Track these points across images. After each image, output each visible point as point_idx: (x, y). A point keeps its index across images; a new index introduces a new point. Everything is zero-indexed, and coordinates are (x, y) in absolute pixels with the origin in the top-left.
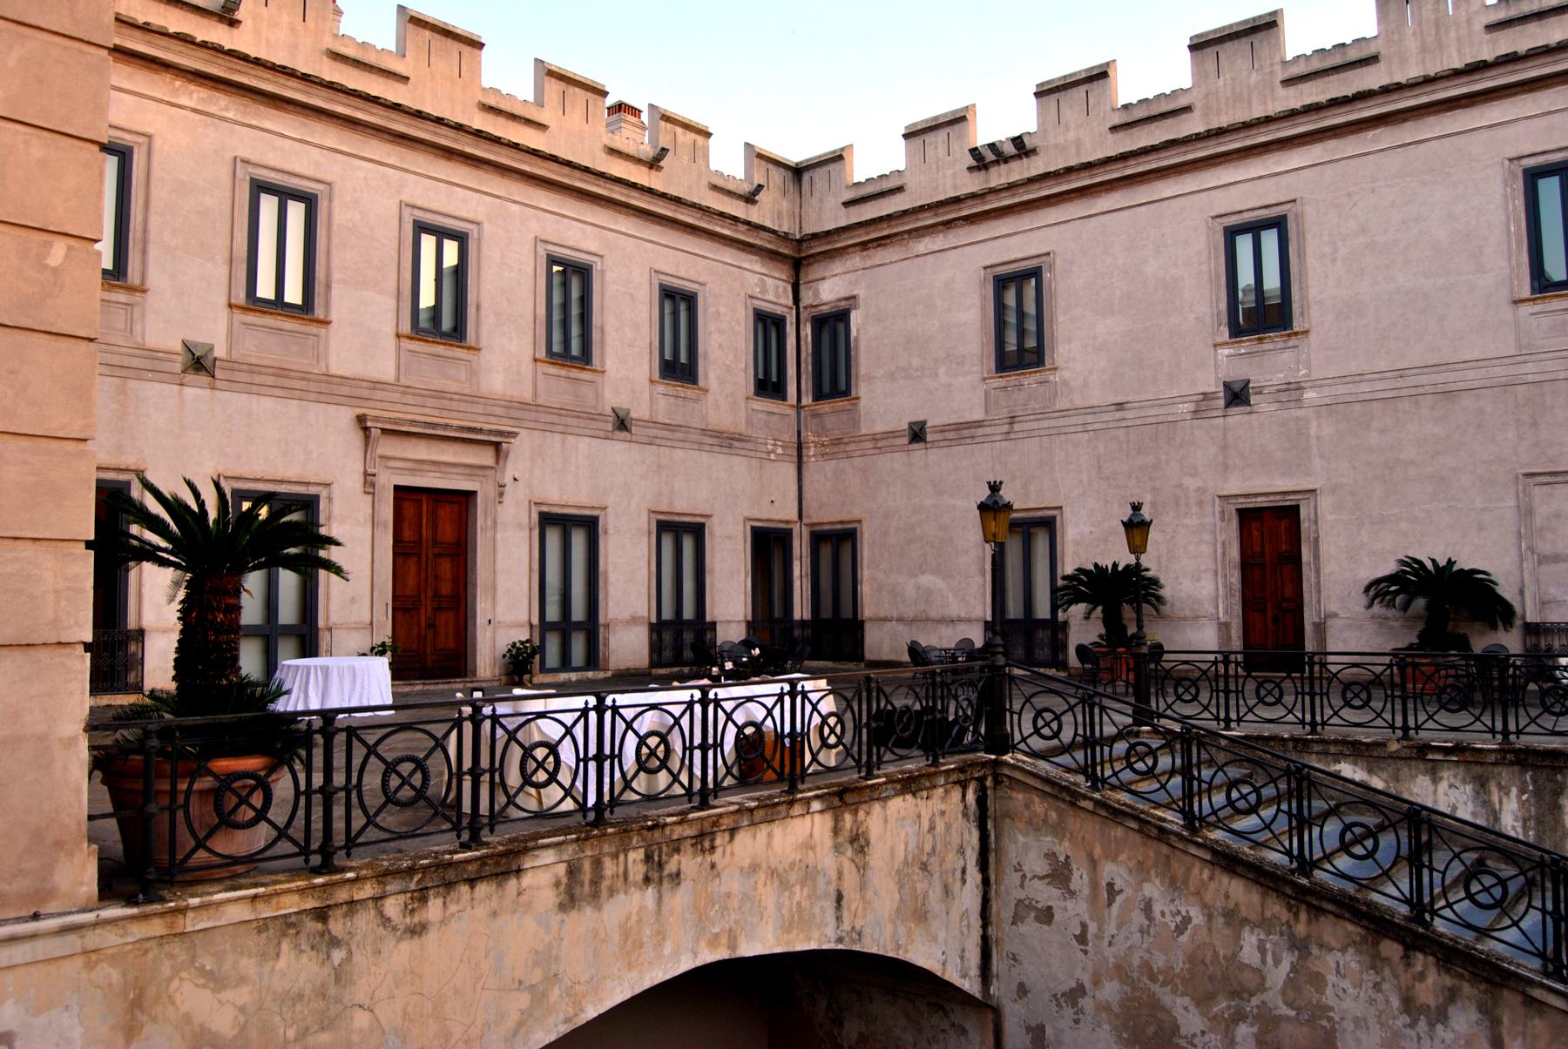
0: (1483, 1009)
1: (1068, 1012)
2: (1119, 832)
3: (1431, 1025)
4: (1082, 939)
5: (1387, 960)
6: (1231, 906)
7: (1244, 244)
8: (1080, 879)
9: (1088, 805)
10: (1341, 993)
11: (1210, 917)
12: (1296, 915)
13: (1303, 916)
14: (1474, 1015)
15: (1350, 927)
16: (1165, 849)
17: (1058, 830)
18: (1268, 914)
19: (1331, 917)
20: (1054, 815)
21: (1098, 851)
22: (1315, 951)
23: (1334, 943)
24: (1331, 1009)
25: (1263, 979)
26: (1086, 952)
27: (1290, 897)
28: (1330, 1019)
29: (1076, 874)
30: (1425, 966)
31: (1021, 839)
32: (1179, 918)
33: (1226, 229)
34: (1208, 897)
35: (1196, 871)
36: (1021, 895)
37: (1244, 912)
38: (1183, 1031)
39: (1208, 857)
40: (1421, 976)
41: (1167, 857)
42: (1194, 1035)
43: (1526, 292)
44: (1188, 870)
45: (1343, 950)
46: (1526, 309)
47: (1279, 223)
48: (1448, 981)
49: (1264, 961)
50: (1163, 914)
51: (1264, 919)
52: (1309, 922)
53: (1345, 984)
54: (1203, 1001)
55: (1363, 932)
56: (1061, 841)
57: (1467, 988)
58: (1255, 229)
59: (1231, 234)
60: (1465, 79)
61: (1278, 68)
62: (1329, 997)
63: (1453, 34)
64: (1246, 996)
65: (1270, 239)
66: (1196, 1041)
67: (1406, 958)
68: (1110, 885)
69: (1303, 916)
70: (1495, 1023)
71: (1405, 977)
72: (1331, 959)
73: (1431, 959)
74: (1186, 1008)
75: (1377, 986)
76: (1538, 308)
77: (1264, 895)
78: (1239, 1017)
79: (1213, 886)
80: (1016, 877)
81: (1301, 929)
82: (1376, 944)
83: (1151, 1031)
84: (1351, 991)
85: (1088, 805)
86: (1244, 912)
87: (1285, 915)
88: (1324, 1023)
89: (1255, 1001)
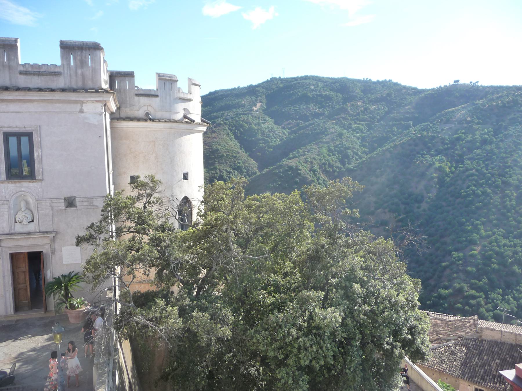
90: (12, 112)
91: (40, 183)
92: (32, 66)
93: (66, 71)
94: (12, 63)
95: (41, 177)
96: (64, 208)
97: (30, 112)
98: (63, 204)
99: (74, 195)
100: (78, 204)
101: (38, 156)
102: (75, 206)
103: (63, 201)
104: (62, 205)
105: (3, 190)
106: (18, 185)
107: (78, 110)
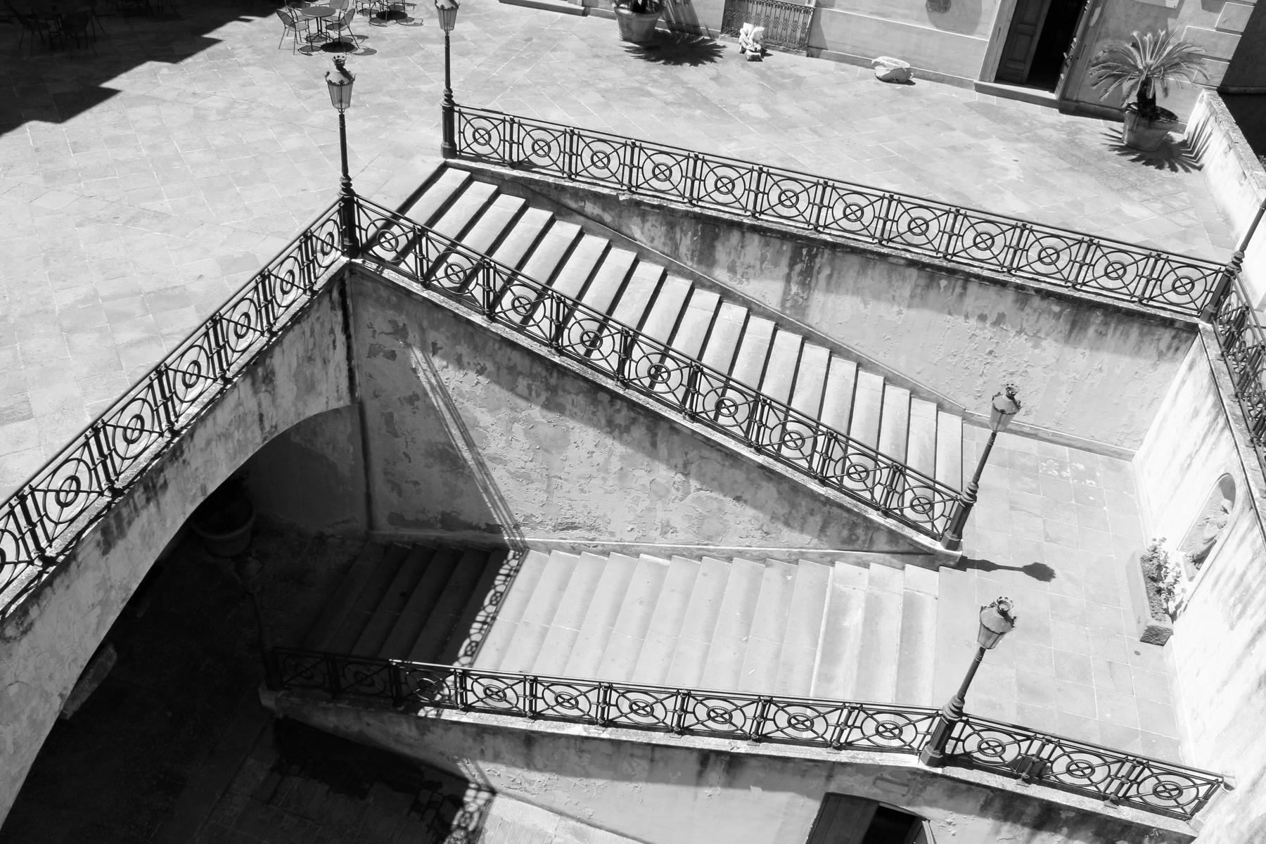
0: (648, 428)
1: (408, 408)
3: (621, 433)
5: (601, 402)
6: (512, 364)
11: (499, 369)
12: (551, 374)
13: (555, 375)
14: (643, 430)
21: (425, 324)
22: (560, 393)
31: (371, 310)
34: (497, 359)
35: (490, 343)
36: (373, 341)
37: (519, 369)
40: (619, 411)
45: (577, 394)
48: (632, 414)
57: (642, 419)
69: (555, 375)
70: (654, 435)
71: (610, 411)
72: (569, 398)
75: (594, 413)
78: (514, 420)
79: (500, 353)
80: (370, 332)
81: (553, 381)
82: (596, 393)
86: (519, 369)
87: (544, 373)
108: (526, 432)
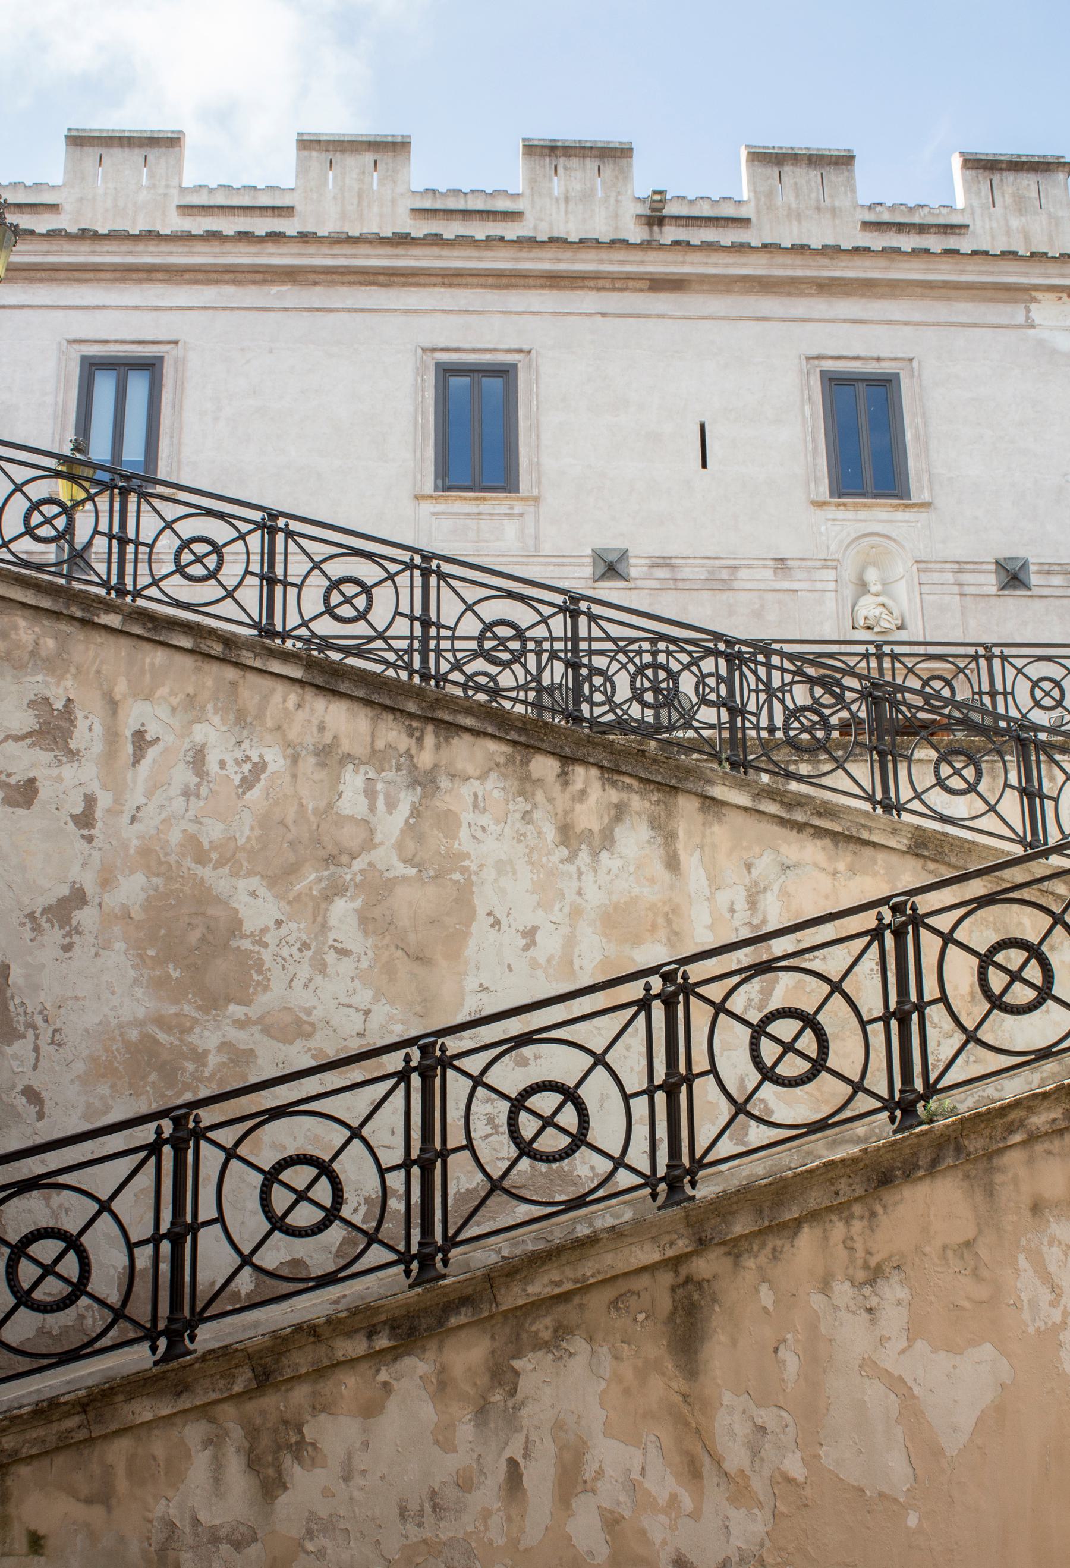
0: (655, 824)
1: (54, 936)
2: (159, 657)
3: (595, 854)
4: (85, 820)
6: (328, 738)
7: (105, 387)
8: (88, 733)
9: (113, 620)
10: (479, 834)
11: (295, 759)
12: (420, 740)
13: (430, 740)
14: (644, 832)
15: (492, 746)
16: (231, 673)
17: (55, 665)
18: (380, 744)
19: (467, 737)
20: (50, 643)
21: (121, 688)
22: (444, 783)
23: (471, 770)
24: (467, 856)
25: (372, 832)
26: (90, 839)
27: (411, 716)
28: (464, 870)
29: (81, 724)
30: (587, 782)
32: (247, 768)
33: (84, 358)
34: (293, 734)
35: (277, 697)
37: (346, 746)
38: (248, 927)
39: (297, 673)
40: (583, 792)
41: (234, 684)
42: (264, 930)
43: (429, 488)
44: (266, 698)
45: (483, 777)
46: (427, 507)
47: (151, 367)
48: (614, 796)
49: (372, 808)
50: (222, 764)
51: (374, 752)
52: (438, 747)
53: (485, 820)
54: (280, 878)
55: (507, 749)
56: (61, 678)
57: (636, 802)
58: (122, 367)
59: (92, 367)
60: (389, 250)
61: (175, 192)
62: (464, 841)
63: (375, 209)
64: (345, 859)
65: (138, 387)
66: (267, 938)
67: (564, 777)
68: (139, 735)
69: (430, 740)
70: (670, 837)
71: (562, 800)
72: (466, 791)
73: (594, 772)
74: (253, 894)
75: (526, 817)
76: (440, 508)
77: (375, 720)
78: (335, 890)
79: (301, 716)
81: (426, 758)
82: (526, 762)
83: (194, 937)
84: (493, 828)
85: (113, 620)
86: (346, 746)
87: (404, 742)
88: (457, 876)
89: (358, 865)
90: (845, 321)
91: (923, 515)
92: (893, 208)
93: (979, 223)
94: (842, 202)
95: (926, 497)
96: (994, 590)
97: (890, 323)
98: (992, 579)
99: (1021, 553)
100: (1034, 579)
101: (917, 437)
102: (1028, 587)
103: (993, 567)
104: (990, 581)
105: (823, 528)
106: (862, 514)
107: (1021, 319)
108: (364, 920)
